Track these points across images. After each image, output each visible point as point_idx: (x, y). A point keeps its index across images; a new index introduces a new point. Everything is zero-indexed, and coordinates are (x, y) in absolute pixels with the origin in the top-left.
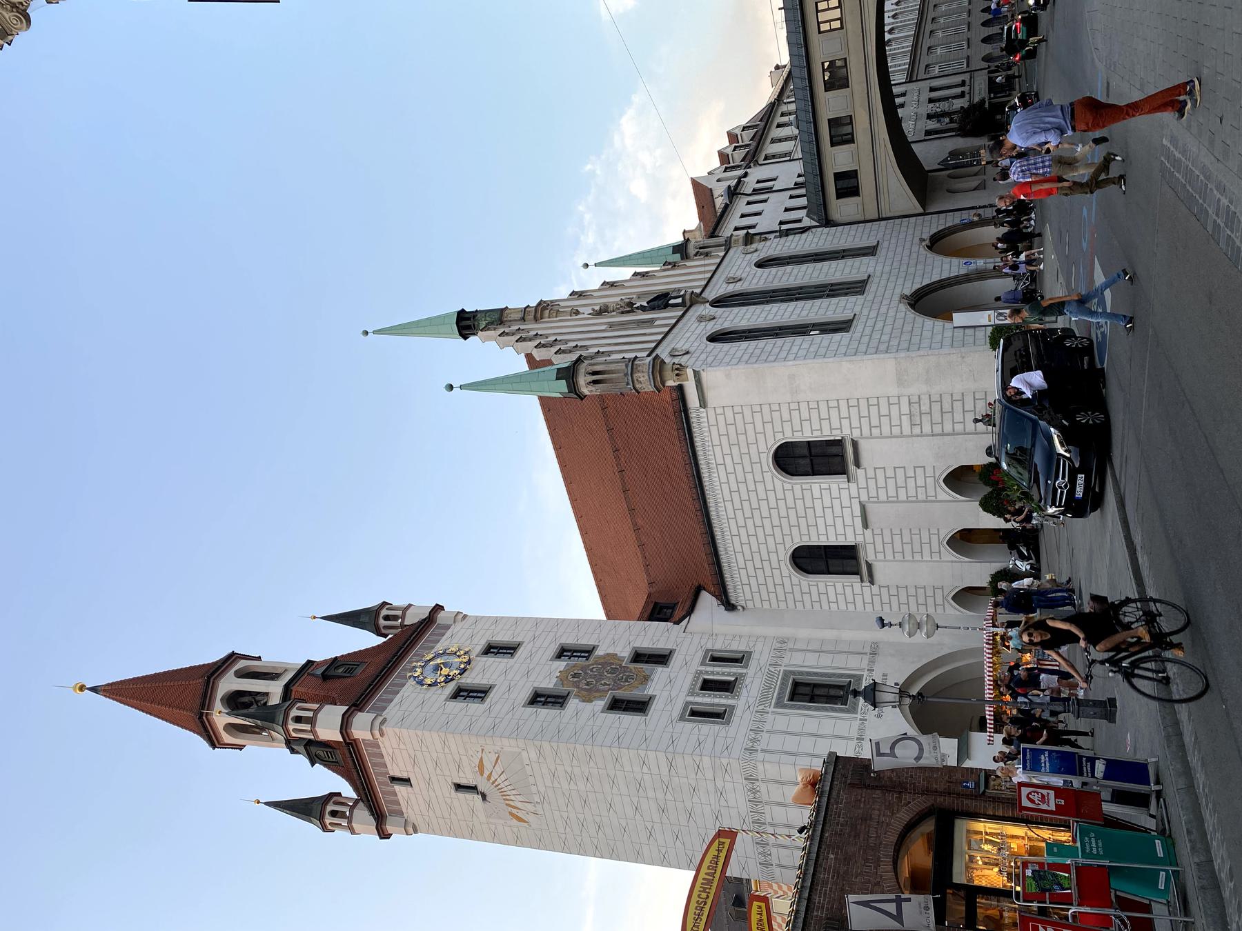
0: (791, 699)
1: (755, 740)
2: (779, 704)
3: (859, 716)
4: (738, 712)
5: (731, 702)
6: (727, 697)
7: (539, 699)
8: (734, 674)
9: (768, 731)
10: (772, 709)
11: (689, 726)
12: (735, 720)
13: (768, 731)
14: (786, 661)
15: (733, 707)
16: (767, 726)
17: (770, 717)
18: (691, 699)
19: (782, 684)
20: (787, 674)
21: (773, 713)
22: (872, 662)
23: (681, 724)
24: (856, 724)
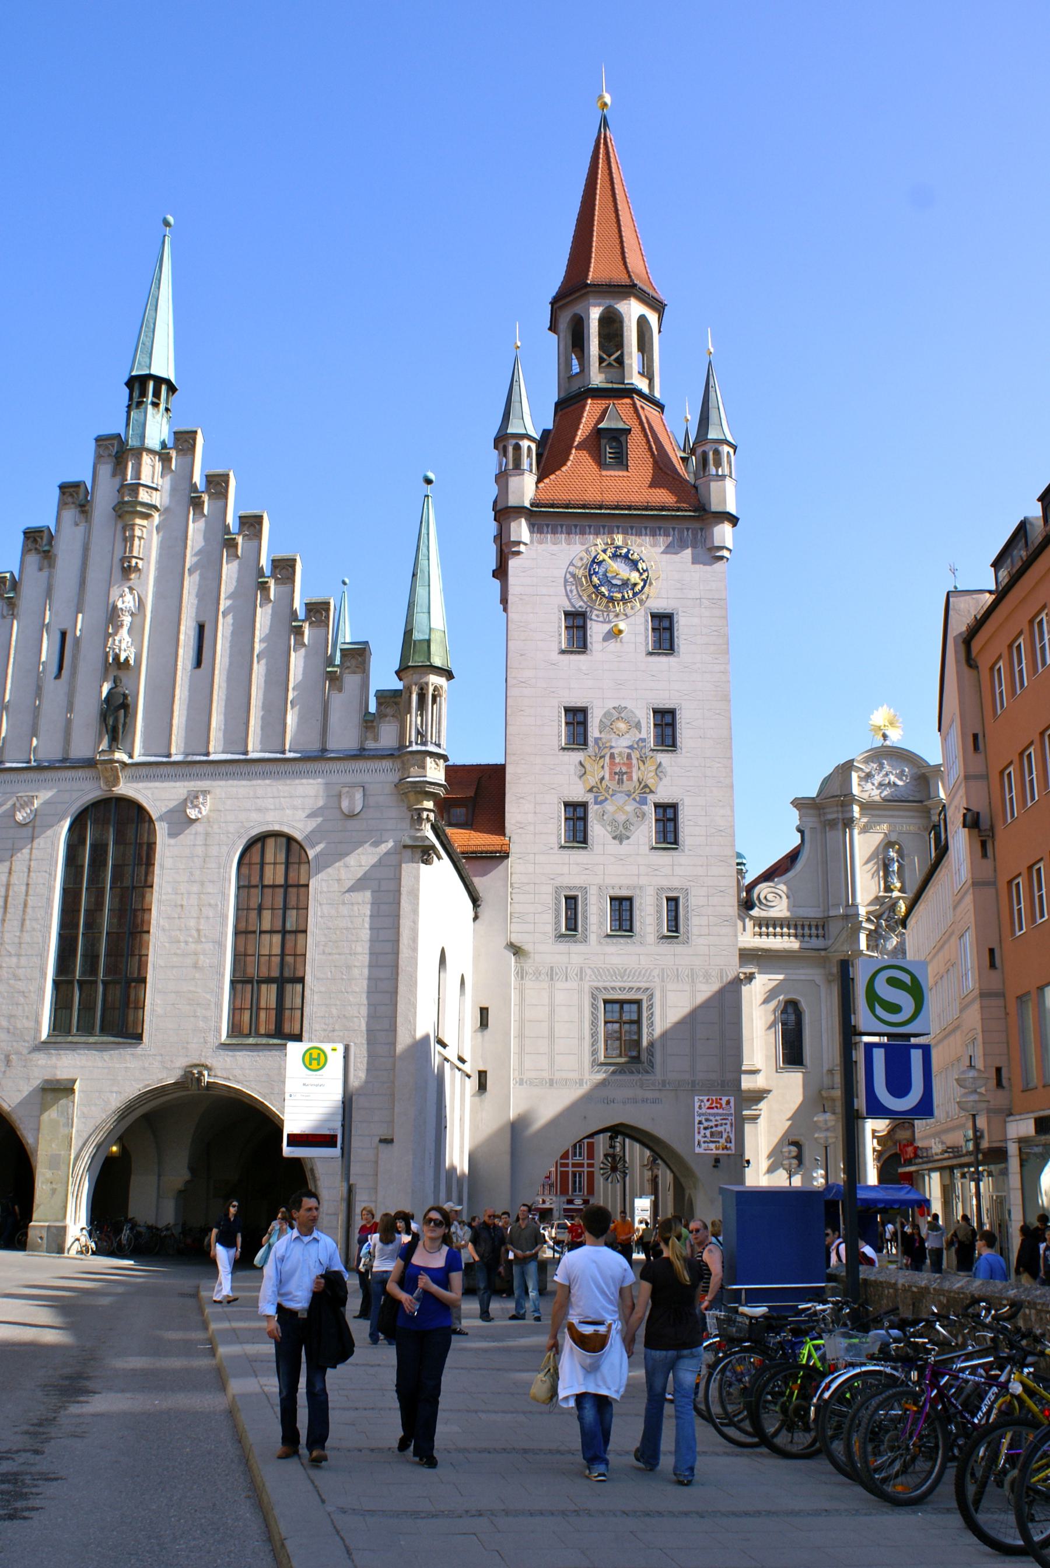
0: (606, 1002)
4: (576, 948)
5: (593, 938)
7: (577, 718)
11: (549, 899)
12: (563, 947)
15: (585, 940)
17: (573, 984)
18: (593, 891)
23: (550, 889)
24: (574, 1075)
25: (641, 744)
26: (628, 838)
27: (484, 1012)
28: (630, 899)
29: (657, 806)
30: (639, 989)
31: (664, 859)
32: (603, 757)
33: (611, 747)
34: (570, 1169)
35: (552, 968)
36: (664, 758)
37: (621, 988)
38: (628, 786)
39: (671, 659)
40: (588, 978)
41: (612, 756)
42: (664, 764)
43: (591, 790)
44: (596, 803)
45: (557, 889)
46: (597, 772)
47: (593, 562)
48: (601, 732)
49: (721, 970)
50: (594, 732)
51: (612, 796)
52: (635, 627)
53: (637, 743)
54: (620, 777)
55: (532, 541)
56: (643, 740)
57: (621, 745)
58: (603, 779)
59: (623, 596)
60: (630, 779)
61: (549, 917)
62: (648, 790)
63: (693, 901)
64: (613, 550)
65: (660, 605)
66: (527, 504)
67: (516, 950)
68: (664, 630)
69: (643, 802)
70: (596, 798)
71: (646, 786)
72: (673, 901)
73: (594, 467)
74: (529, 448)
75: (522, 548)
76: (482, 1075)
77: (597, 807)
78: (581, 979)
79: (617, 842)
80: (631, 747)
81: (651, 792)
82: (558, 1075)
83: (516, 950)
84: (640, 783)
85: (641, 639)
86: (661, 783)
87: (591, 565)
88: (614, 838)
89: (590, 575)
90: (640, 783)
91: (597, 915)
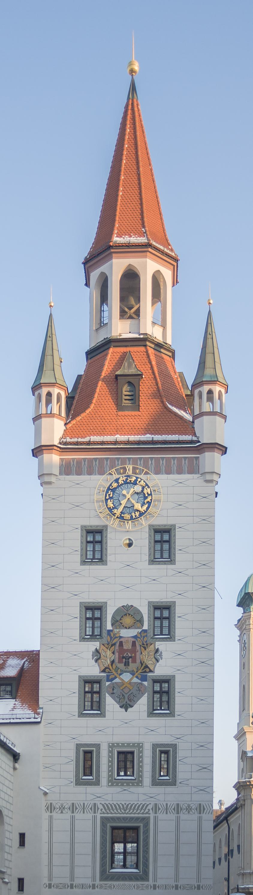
0: (113, 828)
1: (62, 809)
2: (104, 821)
3: (98, 882)
4: (91, 789)
5: (104, 780)
6: (109, 776)
8: (141, 777)
9: (73, 818)
10: (99, 816)
11: (72, 754)
12: (82, 789)
13: (73, 818)
14: (161, 816)
15: (97, 783)
16: (78, 816)
17: (89, 816)
19: (132, 818)
20: (146, 821)
21: (95, 818)
22: (166, 887)
23: (73, 747)
24: (89, 882)
25: (143, 635)
26: (132, 706)
27: (22, 836)
28: (132, 753)
29: (155, 681)
30: (137, 819)
32: (114, 644)
33: (121, 637)
35: (73, 804)
36: (160, 645)
38: (133, 666)
39: (170, 566)
40: (99, 811)
41: (121, 644)
42: (160, 649)
43: (104, 671)
44: (107, 681)
45: (78, 746)
46: (108, 655)
47: (109, 489)
48: (112, 625)
49: (200, 805)
51: (120, 674)
53: (140, 633)
55: (61, 474)
56: (145, 631)
57: (127, 634)
58: (113, 662)
59: (132, 516)
60: (134, 661)
61: (72, 767)
62: (148, 670)
63: (180, 754)
64: (125, 478)
66: (56, 442)
69: (144, 679)
70: (108, 676)
71: (147, 667)
73: (114, 407)
74: (59, 396)
75: (53, 479)
76: (21, 881)
77: (108, 683)
78: (95, 813)
79: (123, 710)
80: (135, 637)
81: (151, 671)
82: (76, 882)
84: (142, 664)
85: (146, 550)
86: (158, 664)
87: (107, 492)
88: (121, 707)
89: (106, 500)
90: (142, 664)
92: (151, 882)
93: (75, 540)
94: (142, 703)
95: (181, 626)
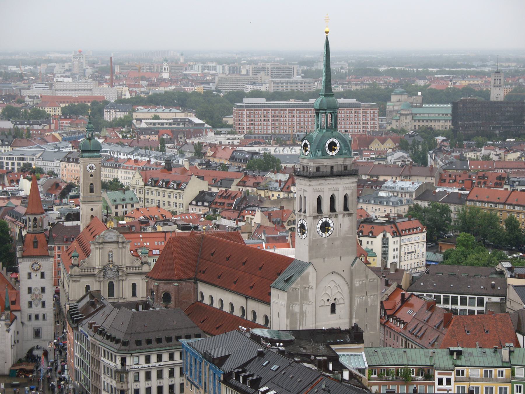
7: (30, 289)
31: (43, 309)
34: (57, 278)
36: (43, 294)
37: (37, 327)
46: (34, 297)
50: (33, 291)
52: (39, 275)
54: (37, 297)
57: (37, 293)
65: (42, 271)
67: (22, 323)
68: (43, 275)
72: (44, 315)
83: (22, 323)
91: (33, 317)
92: (42, 339)
93: (26, 276)
94: (40, 305)
95: (46, 291)
